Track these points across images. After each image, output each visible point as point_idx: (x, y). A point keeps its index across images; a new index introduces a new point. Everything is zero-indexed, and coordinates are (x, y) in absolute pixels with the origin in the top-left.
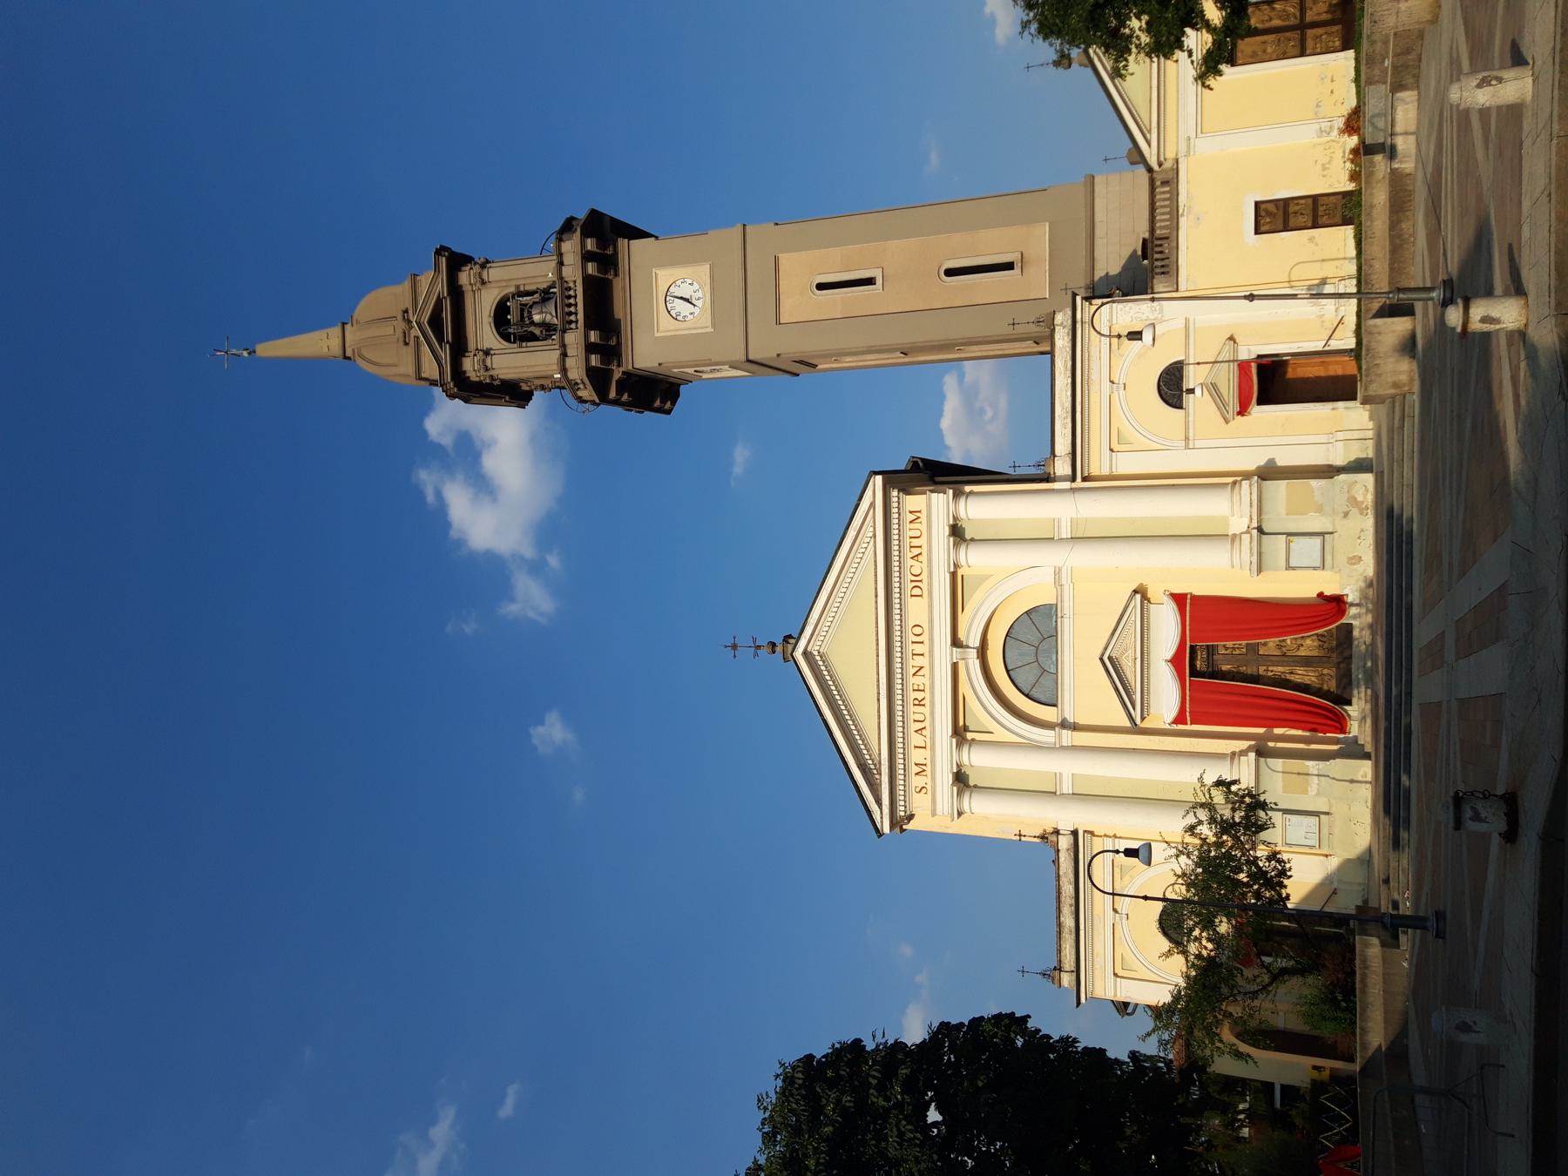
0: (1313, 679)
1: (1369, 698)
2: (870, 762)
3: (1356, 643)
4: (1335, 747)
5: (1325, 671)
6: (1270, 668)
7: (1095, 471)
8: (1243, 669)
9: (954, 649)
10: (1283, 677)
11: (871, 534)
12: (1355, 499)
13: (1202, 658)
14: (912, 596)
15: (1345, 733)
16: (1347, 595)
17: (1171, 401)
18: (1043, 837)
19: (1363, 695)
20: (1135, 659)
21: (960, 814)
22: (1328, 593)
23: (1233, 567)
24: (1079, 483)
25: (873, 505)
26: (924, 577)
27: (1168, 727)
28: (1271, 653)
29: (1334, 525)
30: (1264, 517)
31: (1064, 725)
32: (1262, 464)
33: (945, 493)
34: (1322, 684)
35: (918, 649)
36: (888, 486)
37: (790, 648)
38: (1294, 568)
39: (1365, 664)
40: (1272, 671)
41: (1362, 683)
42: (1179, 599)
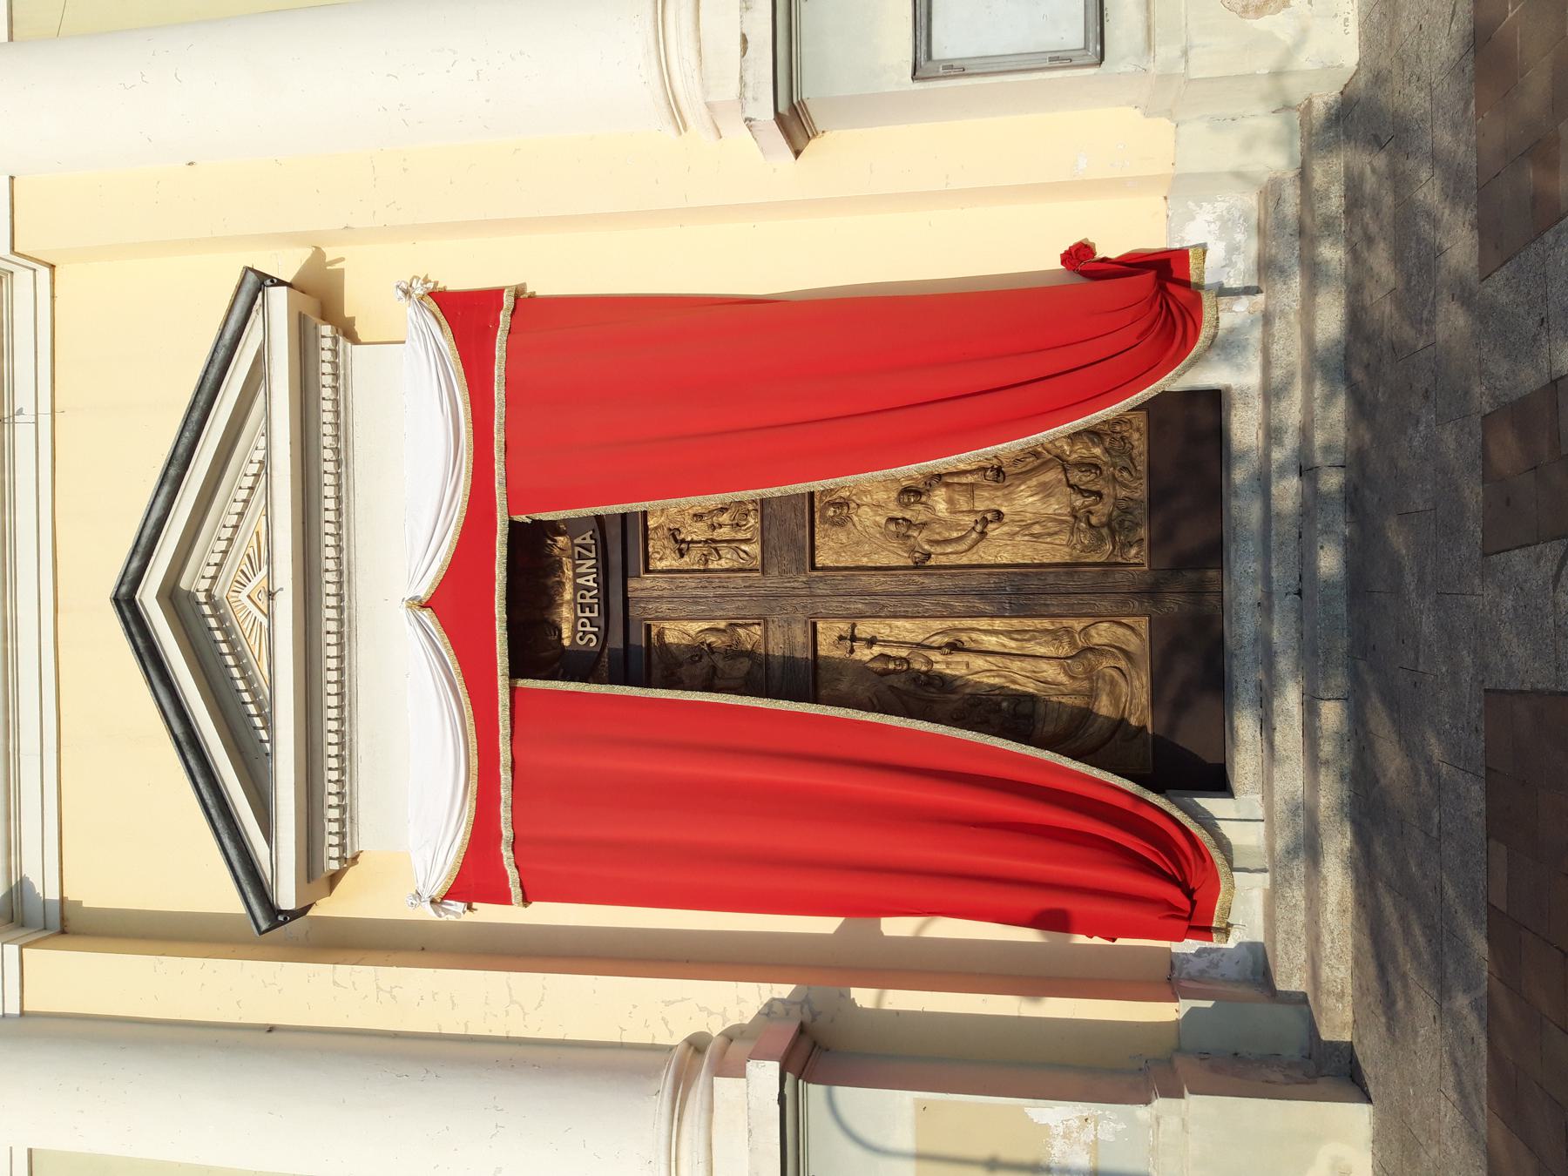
0: (1051, 671)
6: (865, 628)
8: (751, 636)
13: (577, 587)
15: (1205, 931)
16: (1203, 249)
19: (1290, 735)
22: (1110, 248)
27: (427, 913)
28: (865, 561)
34: (1092, 694)
38: (955, 70)
40: (872, 642)
41: (1284, 664)
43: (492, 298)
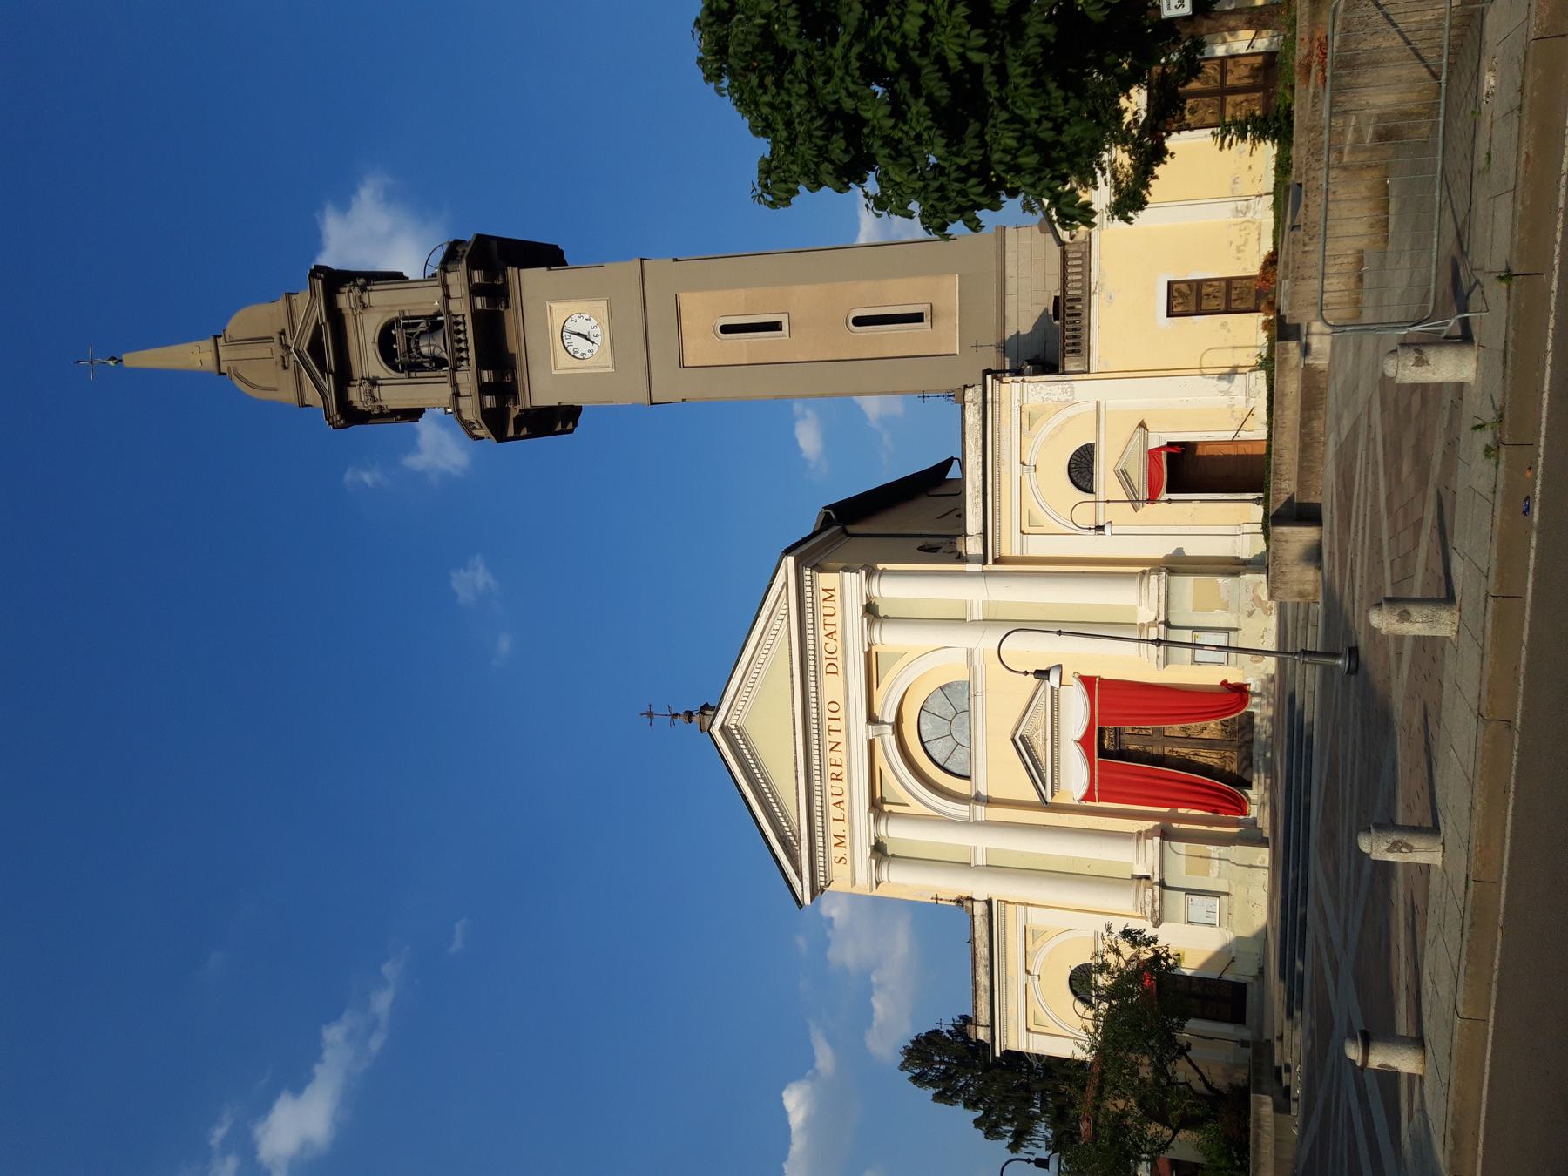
0: (1216, 761)
1: (1267, 787)
2: (790, 834)
3: (1257, 730)
4: (1236, 830)
5: (1227, 754)
6: (1175, 749)
7: (1006, 552)
9: (870, 726)
10: (1187, 757)
11: (784, 612)
12: (1260, 598)
14: (827, 673)
15: (1245, 815)
16: (1249, 684)
17: (1084, 486)
18: (959, 901)
19: (1262, 780)
20: (1046, 740)
21: (878, 884)
23: (1140, 656)
24: (990, 566)
25: (786, 584)
26: (839, 654)
27: (1077, 803)
28: (1176, 735)
29: (1239, 622)
30: (1171, 611)
31: (978, 799)
32: (1170, 552)
33: (858, 573)
34: (1225, 766)
35: (835, 725)
36: (800, 566)
37: (707, 720)
39: (1265, 752)
41: (1261, 770)
42: (1088, 682)
43: (1093, 678)
